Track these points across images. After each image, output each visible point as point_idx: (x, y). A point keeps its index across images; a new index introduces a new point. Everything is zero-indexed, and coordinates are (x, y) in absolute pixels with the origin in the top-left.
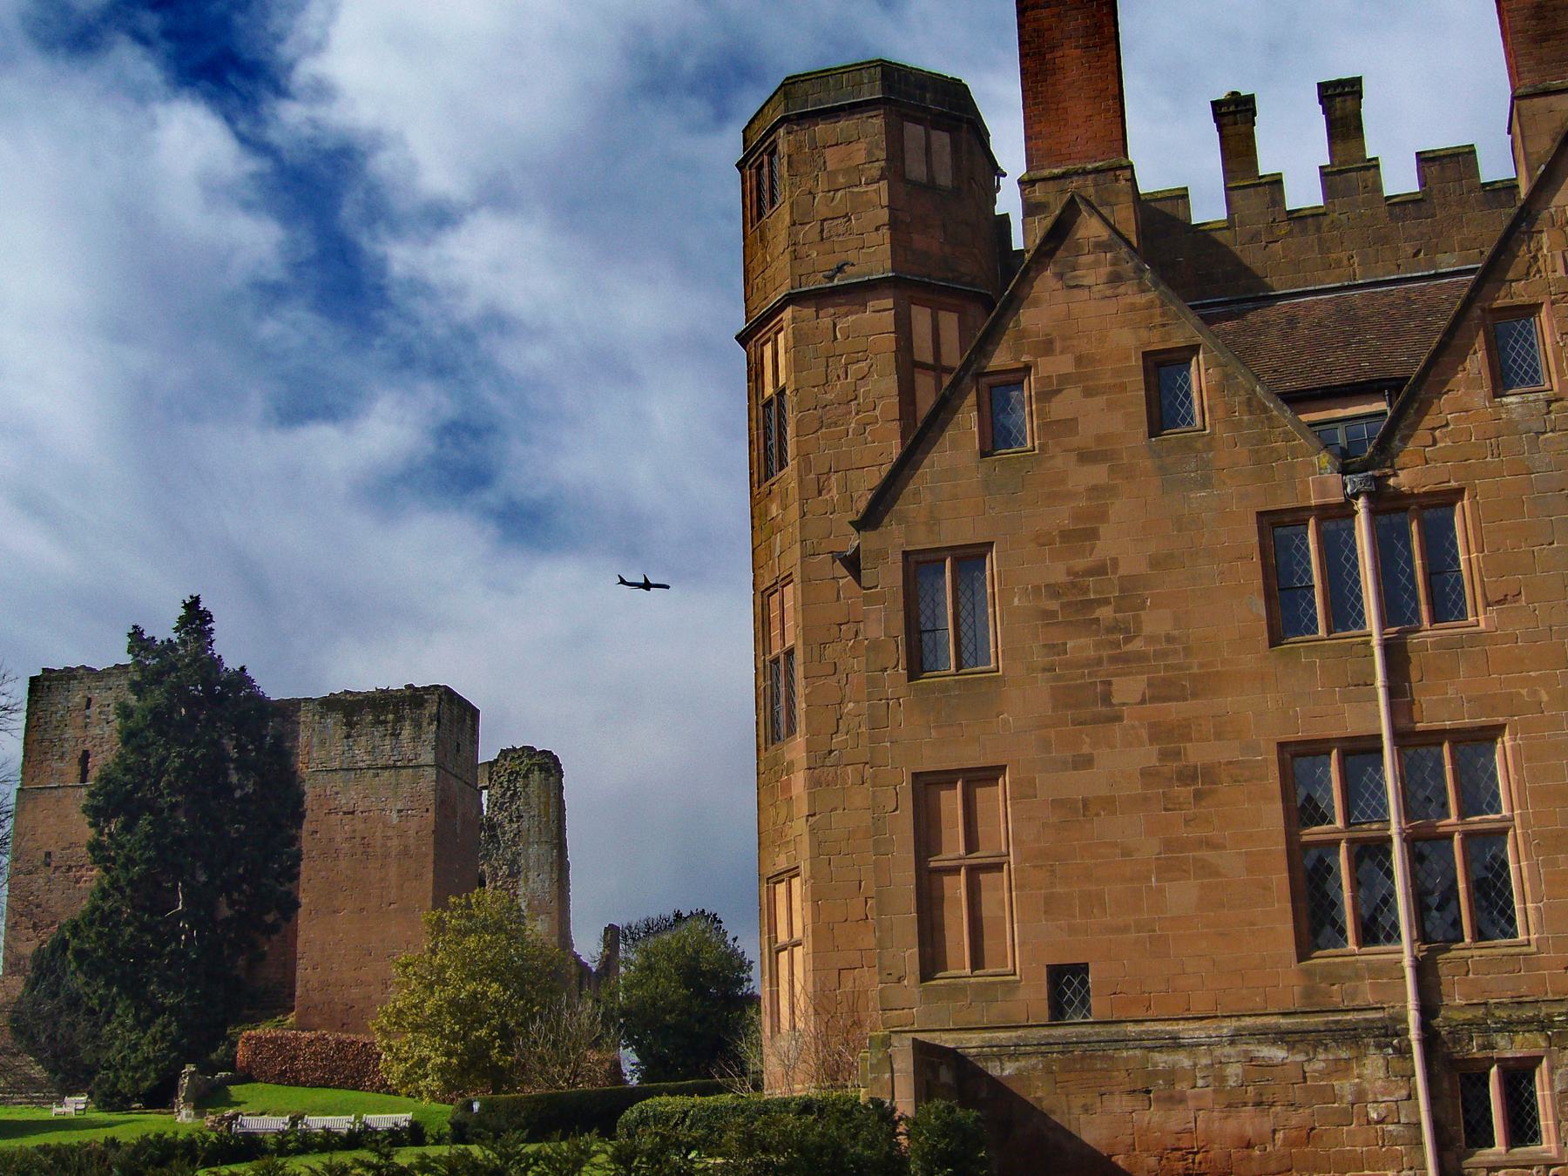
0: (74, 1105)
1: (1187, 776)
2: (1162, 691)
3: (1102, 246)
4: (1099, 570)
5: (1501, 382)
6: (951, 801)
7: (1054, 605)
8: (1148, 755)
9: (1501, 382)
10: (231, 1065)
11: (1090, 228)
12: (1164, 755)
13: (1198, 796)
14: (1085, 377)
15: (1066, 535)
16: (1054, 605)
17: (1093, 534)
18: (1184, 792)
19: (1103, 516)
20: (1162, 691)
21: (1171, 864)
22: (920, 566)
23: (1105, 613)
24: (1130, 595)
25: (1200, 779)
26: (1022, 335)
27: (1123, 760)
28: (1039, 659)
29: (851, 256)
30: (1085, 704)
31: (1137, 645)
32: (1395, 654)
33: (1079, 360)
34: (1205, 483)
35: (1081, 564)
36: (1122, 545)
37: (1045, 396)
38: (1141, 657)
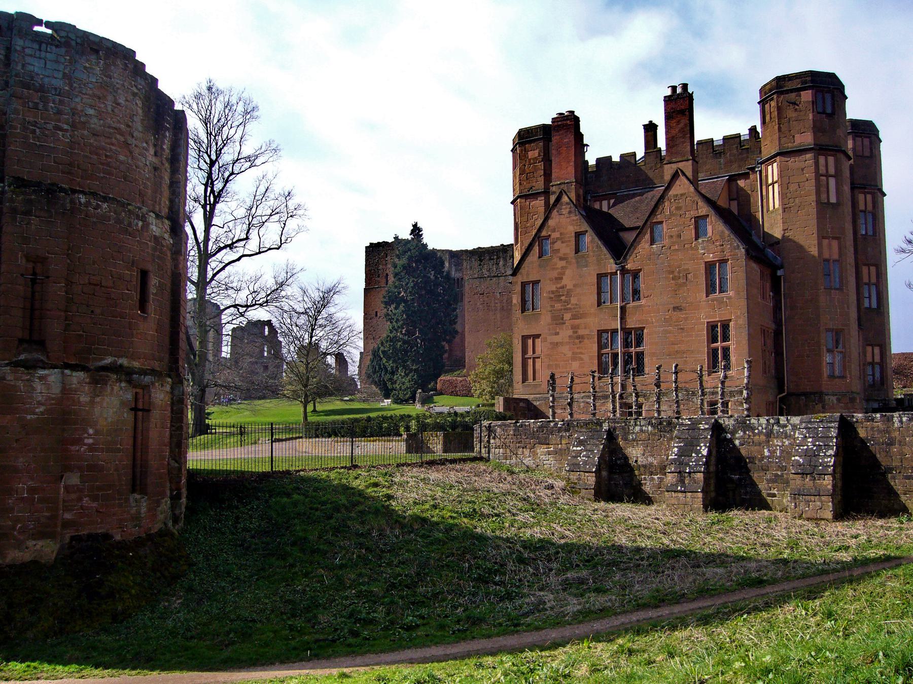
0: (387, 402)
1: (579, 337)
2: (574, 317)
3: (567, 203)
4: (563, 287)
5: (652, 242)
6: (530, 342)
7: (552, 296)
8: (570, 332)
9: (652, 242)
10: (435, 390)
11: (565, 199)
12: (574, 332)
14: (562, 239)
15: (556, 279)
16: (552, 296)
17: (562, 278)
19: (564, 274)
20: (574, 317)
21: (574, 359)
22: (524, 285)
23: (563, 298)
24: (569, 295)
25: (581, 338)
26: (549, 227)
27: (565, 333)
28: (549, 309)
30: (558, 320)
32: (623, 309)
33: (561, 234)
34: (586, 266)
35: (559, 286)
36: (567, 281)
37: (553, 243)
38: (570, 309)
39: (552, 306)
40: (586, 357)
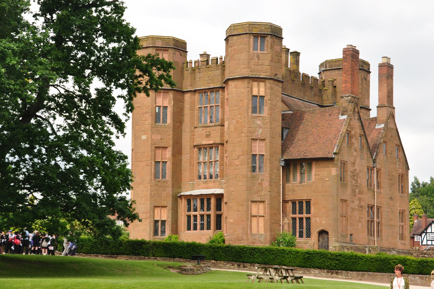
1: (361, 207)
4: (355, 170)
12: (360, 203)
13: (362, 210)
16: (352, 175)
18: (360, 209)
23: (355, 177)
26: (350, 125)
29: (278, 73)
31: (358, 184)
33: (355, 133)
35: (354, 168)
40: (363, 220)
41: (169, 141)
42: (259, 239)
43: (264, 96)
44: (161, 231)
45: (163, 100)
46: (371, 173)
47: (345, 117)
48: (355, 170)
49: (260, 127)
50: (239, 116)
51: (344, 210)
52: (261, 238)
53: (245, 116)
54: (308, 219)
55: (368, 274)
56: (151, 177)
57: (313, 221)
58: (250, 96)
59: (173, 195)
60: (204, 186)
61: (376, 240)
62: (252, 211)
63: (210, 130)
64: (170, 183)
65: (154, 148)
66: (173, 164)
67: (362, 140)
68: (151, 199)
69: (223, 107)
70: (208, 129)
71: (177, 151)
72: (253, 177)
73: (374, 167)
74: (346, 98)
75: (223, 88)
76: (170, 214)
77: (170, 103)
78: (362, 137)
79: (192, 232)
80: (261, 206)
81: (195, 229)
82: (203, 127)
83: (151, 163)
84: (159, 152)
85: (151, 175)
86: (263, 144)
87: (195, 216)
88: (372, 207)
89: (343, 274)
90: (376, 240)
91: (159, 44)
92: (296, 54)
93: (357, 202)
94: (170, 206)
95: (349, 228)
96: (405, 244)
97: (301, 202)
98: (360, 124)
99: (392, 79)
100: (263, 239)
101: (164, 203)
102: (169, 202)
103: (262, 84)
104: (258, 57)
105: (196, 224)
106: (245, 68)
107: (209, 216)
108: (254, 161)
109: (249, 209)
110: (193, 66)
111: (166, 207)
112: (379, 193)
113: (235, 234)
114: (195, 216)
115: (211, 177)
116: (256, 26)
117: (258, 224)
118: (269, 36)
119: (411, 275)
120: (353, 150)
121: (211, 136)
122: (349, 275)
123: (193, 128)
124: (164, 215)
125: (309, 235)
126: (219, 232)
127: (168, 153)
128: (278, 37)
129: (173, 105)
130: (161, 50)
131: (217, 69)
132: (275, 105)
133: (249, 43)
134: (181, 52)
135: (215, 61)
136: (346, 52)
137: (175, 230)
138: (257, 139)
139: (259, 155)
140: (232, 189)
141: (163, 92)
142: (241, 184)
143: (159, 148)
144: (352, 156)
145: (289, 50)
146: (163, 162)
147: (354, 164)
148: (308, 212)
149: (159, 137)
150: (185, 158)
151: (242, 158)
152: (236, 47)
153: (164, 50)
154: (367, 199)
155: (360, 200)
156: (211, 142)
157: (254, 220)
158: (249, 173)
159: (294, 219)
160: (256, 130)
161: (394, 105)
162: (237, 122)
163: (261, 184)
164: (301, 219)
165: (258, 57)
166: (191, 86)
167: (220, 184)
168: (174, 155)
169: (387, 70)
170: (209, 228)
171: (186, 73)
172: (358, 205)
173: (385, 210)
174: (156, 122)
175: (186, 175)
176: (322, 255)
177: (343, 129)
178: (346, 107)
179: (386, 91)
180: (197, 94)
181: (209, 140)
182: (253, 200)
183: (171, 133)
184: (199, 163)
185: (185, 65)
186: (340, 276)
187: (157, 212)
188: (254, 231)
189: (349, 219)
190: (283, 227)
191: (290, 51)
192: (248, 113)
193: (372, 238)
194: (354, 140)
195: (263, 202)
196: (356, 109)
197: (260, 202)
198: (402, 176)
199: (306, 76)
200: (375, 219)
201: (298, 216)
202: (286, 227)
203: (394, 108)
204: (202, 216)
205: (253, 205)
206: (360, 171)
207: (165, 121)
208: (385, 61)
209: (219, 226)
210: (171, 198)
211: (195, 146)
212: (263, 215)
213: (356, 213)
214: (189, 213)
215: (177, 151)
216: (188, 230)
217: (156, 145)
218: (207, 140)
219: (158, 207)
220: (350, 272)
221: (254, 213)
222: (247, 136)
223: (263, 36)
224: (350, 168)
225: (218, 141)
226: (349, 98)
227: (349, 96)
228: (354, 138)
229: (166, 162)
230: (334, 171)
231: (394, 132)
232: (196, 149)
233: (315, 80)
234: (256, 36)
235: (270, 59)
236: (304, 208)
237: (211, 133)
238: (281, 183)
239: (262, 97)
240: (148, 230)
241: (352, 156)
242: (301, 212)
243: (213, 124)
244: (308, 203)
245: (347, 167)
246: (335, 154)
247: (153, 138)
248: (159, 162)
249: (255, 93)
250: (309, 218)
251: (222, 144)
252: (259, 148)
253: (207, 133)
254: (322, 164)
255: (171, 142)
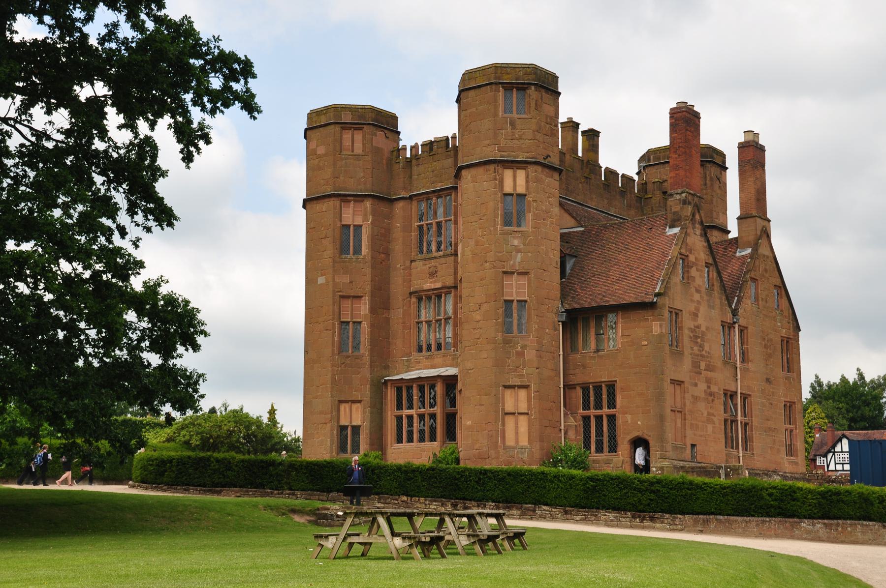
1: (712, 394)
4: (698, 327)
12: (709, 387)
17: (697, 316)
18: (710, 399)
23: (699, 340)
26: (687, 245)
29: (551, 154)
31: (703, 353)
33: (696, 258)
35: (696, 324)
39: (692, 348)
40: (715, 419)
41: (364, 283)
42: (520, 456)
43: (525, 195)
44: (352, 446)
45: (354, 214)
46: (729, 334)
47: (676, 230)
48: (698, 327)
49: (519, 251)
50: (479, 232)
51: (678, 399)
52: (522, 453)
53: (490, 231)
54: (612, 418)
55: (717, 519)
56: (333, 350)
57: (620, 420)
58: (499, 194)
59: (372, 381)
60: (428, 363)
61: (741, 455)
62: (506, 405)
63: (437, 264)
64: (367, 359)
65: (337, 298)
66: (372, 326)
67: (711, 273)
68: (332, 388)
69: (456, 223)
70: (434, 263)
71: (381, 303)
72: (506, 342)
73: (735, 323)
74: (678, 197)
75: (455, 188)
76: (368, 414)
77: (365, 219)
78: (711, 268)
79: (405, 445)
80: (523, 393)
81: (410, 440)
82: (425, 259)
83: (334, 324)
84: (347, 303)
85: (333, 345)
86: (524, 280)
87: (410, 418)
88: (733, 395)
89: (666, 521)
90: (741, 455)
91: (347, 118)
92: (592, 135)
93: (702, 386)
94: (367, 400)
95: (689, 432)
96: (796, 463)
97: (598, 388)
98: (706, 244)
99: (764, 170)
100: (526, 455)
101: (356, 395)
102: (366, 394)
103: (521, 175)
104: (513, 124)
105: (412, 431)
106: (489, 145)
107: (433, 416)
108: (508, 313)
109: (498, 401)
110: (408, 155)
111: (360, 402)
112: (745, 370)
113: (477, 446)
114: (410, 418)
115: (439, 347)
116: (509, 70)
117: (517, 428)
118: (533, 88)
119: (806, 521)
120: (693, 290)
121: (439, 274)
122: (677, 521)
123: (408, 263)
124: (356, 416)
125: (613, 449)
126: (451, 445)
127: (363, 307)
128: (550, 90)
129: (372, 223)
130: (350, 128)
131: (447, 157)
132: (547, 212)
133: (496, 101)
134: (386, 131)
135: (443, 144)
136: (675, 116)
137: (378, 443)
138: (513, 273)
139: (518, 301)
140: (469, 365)
141: (355, 201)
142: (485, 356)
143: (348, 297)
144: (692, 301)
145: (578, 125)
146: (354, 322)
147: (695, 315)
148: (612, 404)
149: (346, 279)
150: (397, 315)
151: (485, 307)
152: (474, 110)
153: (356, 129)
154: (722, 380)
155: (708, 381)
156: (439, 285)
157: (510, 421)
158: (500, 334)
159: (586, 419)
160: (511, 256)
161: (769, 216)
162: (477, 243)
163: (521, 354)
164: (599, 418)
165: (513, 124)
166: (405, 189)
167: (453, 359)
168: (373, 310)
169: (752, 153)
170: (433, 438)
171: (396, 166)
172: (705, 391)
173: (756, 400)
174: (341, 254)
175: (398, 345)
176: (620, 483)
177: (673, 252)
178: (677, 212)
179: (753, 191)
180: (415, 203)
181: (435, 282)
182: (508, 384)
183: (368, 271)
184: (418, 323)
185: (395, 153)
186: (658, 525)
187: (345, 408)
188: (510, 441)
189: (688, 417)
190: (565, 434)
191: (582, 128)
192: (495, 225)
193: (733, 452)
194: (693, 272)
195: (526, 387)
196: (697, 217)
197: (520, 387)
198: (787, 342)
199: (611, 173)
200: (739, 418)
201: (592, 412)
202: (572, 434)
203: (769, 221)
204: (422, 417)
205: (508, 393)
206: (707, 328)
207: (358, 251)
208: (750, 137)
209: (451, 434)
210: (368, 386)
211: (411, 294)
212: (526, 411)
213: (702, 406)
214: (399, 413)
215: (381, 303)
216: (398, 442)
217: (341, 294)
218: (431, 283)
219: (346, 402)
220: (679, 516)
221: (509, 407)
222: (494, 267)
223: (522, 88)
224: (688, 323)
225: (450, 281)
226: (684, 195)
227: (683, 193)
228: (694, 269)
229: (360, 323)
230: (657, 327)
231: (771, 265)
232: (414, 300)
233: (631, 180)
234: (508, 87)
235: (534, 127)
236: (605, 397)
237: (439, 269)
238: (561, 353)
239: (522, 196)
240: (329, 444)
241: (692, 301)
242: (598, 406)
243: (441, 254)
244: (611, 387)
245: (682, 321)
246: (658, 295)
247: (337, 280)
248: (348, 322)
249: (508, 188)
250: (614, 416)
251: (456, 287)
252: (516, 289)
253: (431, 270)
254: (634, 315)
255: (368, 288)
